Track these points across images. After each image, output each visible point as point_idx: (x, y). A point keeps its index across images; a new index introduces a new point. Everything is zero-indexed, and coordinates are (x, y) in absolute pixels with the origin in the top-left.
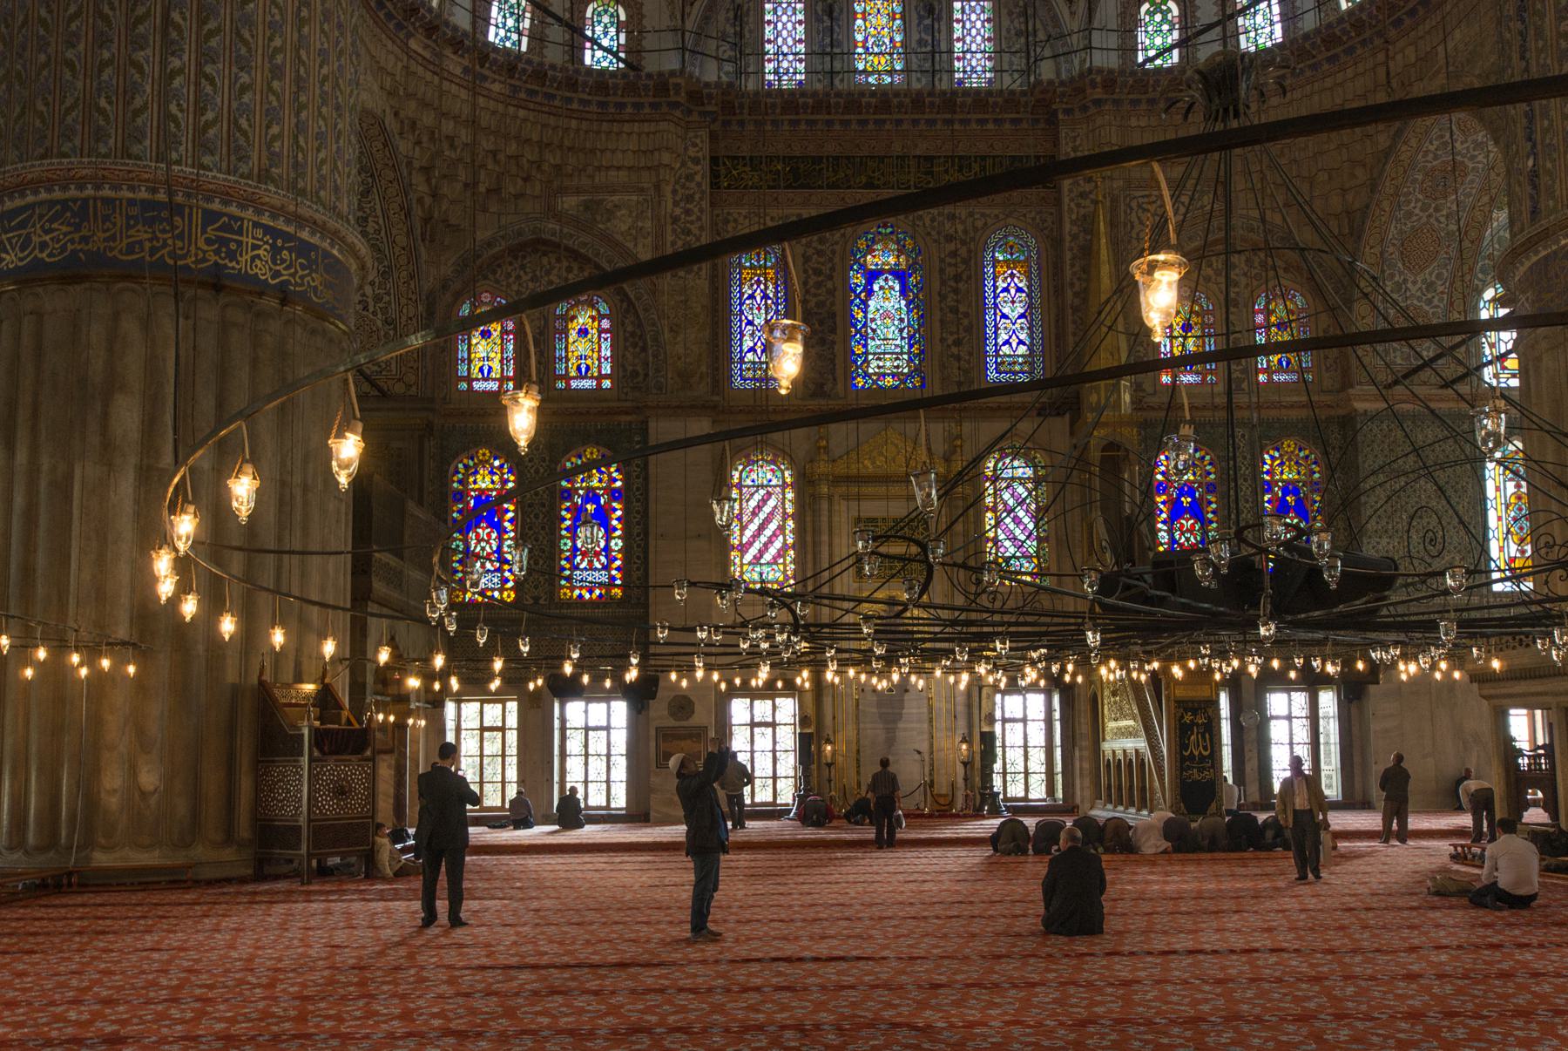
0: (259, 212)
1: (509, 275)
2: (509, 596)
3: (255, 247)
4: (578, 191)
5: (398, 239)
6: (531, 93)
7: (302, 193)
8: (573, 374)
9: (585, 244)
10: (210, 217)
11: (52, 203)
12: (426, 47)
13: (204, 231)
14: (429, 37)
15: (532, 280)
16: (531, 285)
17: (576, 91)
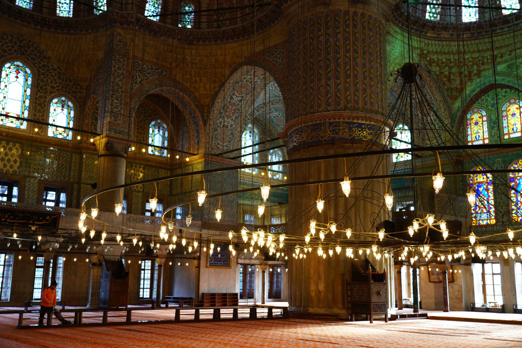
0: (344, 119)
1: (483, 100)
2: (493, 222)
3: (344, 129)
4: (505, 62)
5: (438, 99)
6: (478, 33)
7: (358, 109)
8: (511, 131)
9: (509, 81)
10: (331, 124)
11: (296, 130)
12: (434, 34)
13: (329, 129)
14: (433, 30)
15: (492, 99)
16: (492, 102)
17: (497, 26)
